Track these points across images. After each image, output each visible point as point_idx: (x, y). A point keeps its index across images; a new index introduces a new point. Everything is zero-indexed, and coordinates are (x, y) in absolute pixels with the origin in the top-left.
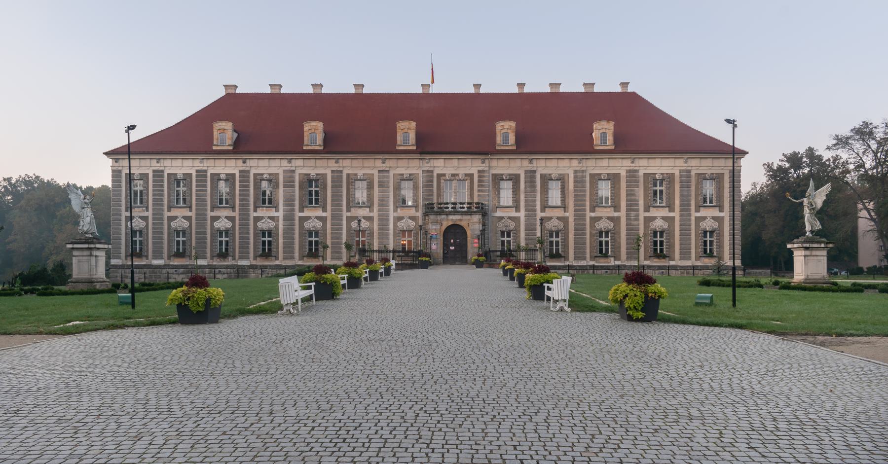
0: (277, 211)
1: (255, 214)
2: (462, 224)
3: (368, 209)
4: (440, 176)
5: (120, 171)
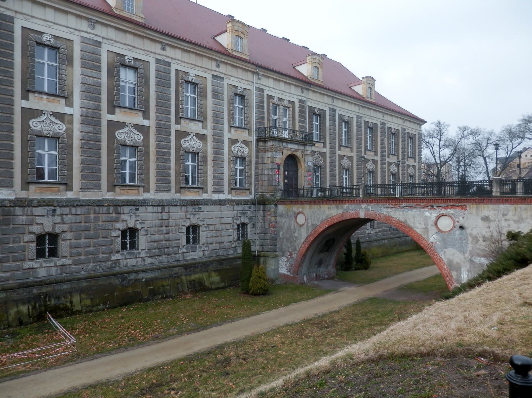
0: (70, 104)
1: (25, 104)
2: (299, 154)
3: (200, 124)
4: (270, 97)
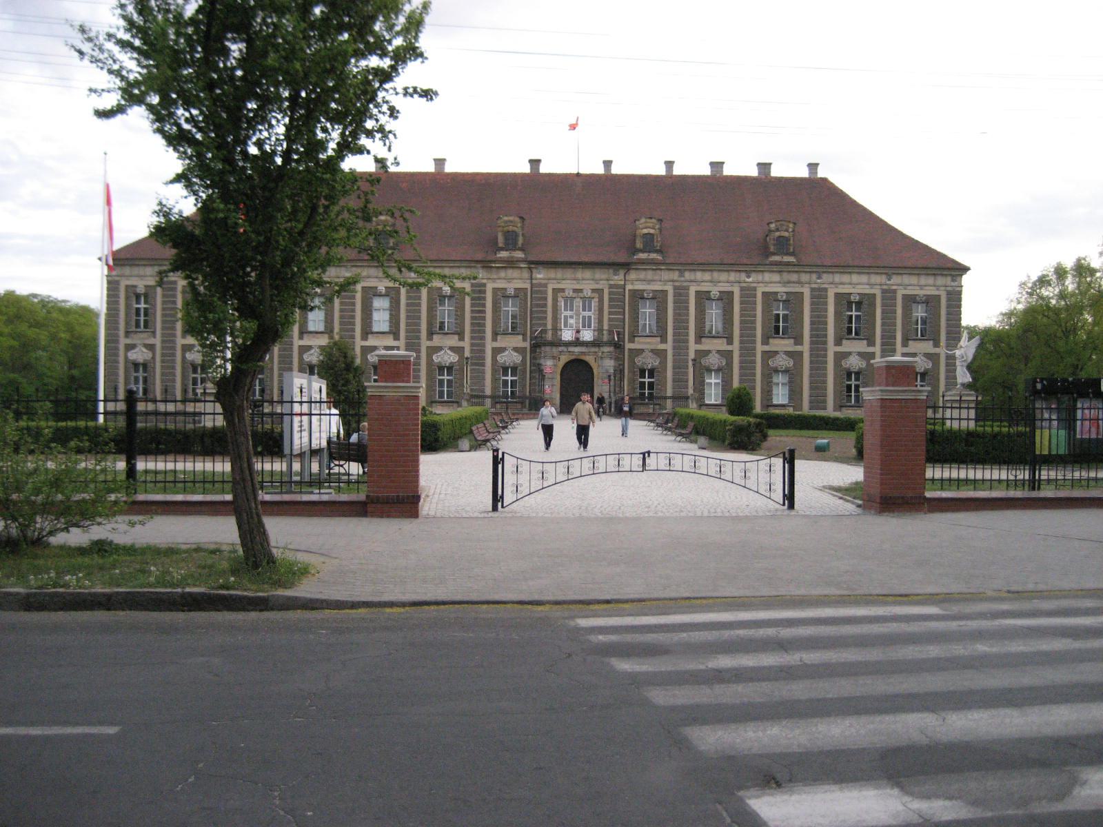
1: (302, 343)
2: (590, 359)
4: (556, 291)
5: (117, 283)
